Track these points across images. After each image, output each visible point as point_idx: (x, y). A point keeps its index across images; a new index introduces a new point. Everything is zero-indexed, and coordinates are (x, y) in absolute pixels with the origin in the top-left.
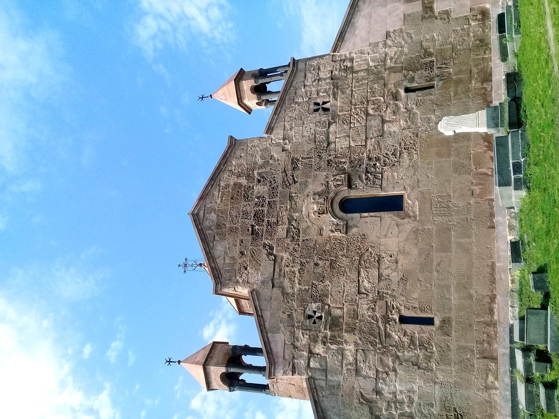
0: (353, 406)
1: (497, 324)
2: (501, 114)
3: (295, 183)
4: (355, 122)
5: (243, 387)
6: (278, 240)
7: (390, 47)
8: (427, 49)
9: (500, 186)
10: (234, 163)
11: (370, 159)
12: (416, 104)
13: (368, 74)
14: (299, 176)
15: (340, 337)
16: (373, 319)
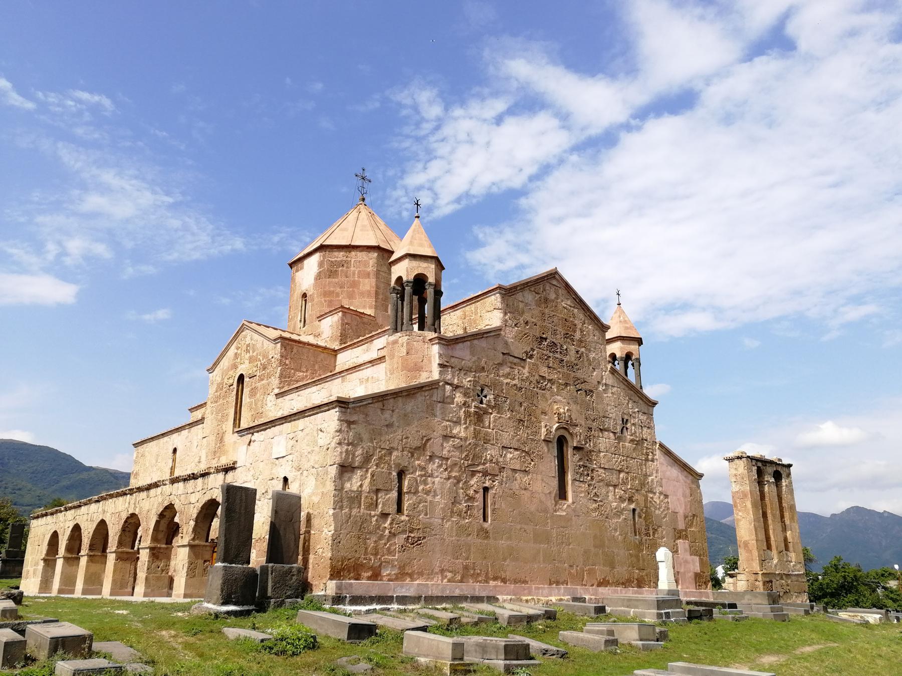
7: (659, 498)
10: (590, 327)
11: (592, 470)
12: (625, 519)
15: (470, 421)
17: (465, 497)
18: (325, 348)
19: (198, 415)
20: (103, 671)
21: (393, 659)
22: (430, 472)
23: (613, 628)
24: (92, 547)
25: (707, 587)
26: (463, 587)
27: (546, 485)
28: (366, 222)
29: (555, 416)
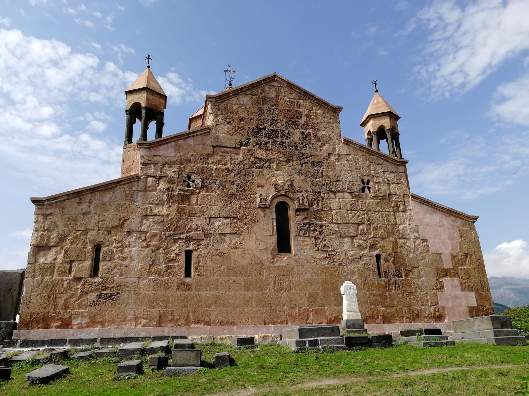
0: (117, 213)
1: (187, 326)
2: (358, 330)
3: (301, 164)
4: (353, 214)
5: (129, 121)
6: (253, 151)
7: (415, 242)
8: (412, 272)
9: (299, 329)
10: (319, 112)
11: (321, 226)
12: (366, 264)
13: (392, 225)
14: (307, 168)
15: (173, 202)
16: (188, 229)
27: (260, 242)
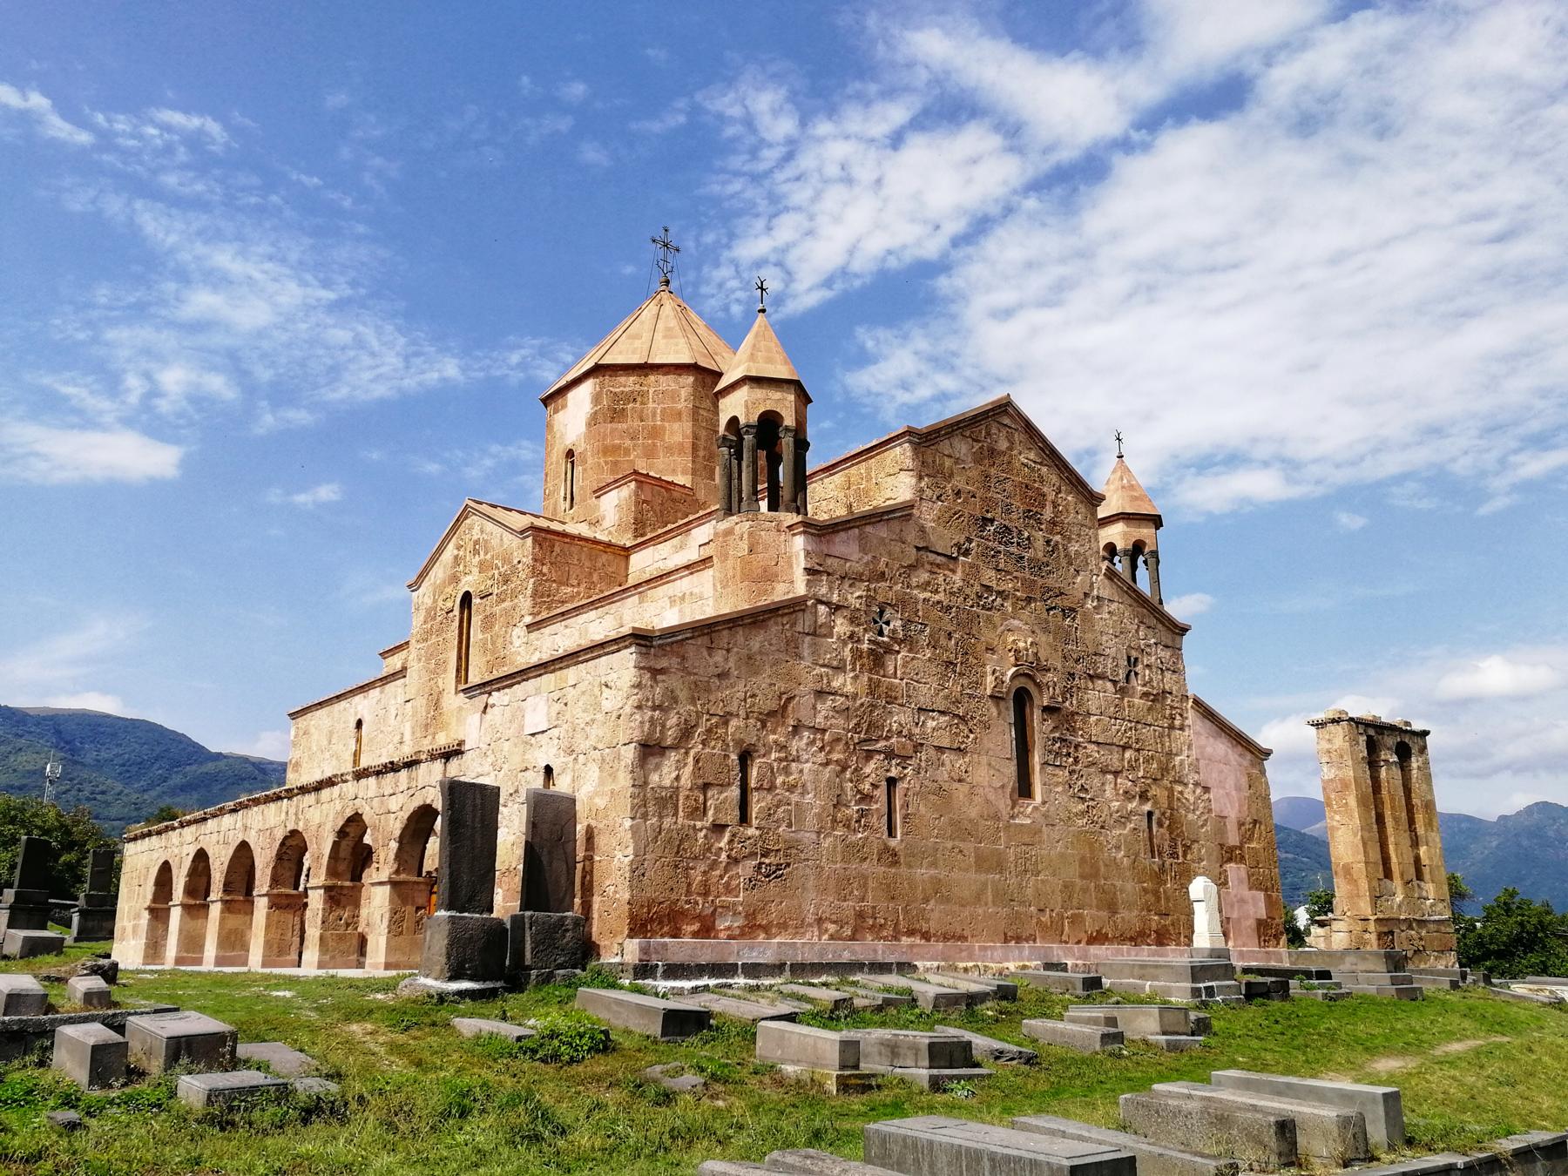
7: (1194, 792)
10: (1069, 498)
12: (1135, 829)
17: (855, 796)
18: (609, 545)
19: (395, 662)
20: (257, 1091)
21: (739, 1067)
22: (795, 753)
23: (1115, 1013)
24: (228, 887)
25: (1278, 944)
26: (857, 948)
27: (997, 774)
28: (673, 323)
29: (1010, 654)
